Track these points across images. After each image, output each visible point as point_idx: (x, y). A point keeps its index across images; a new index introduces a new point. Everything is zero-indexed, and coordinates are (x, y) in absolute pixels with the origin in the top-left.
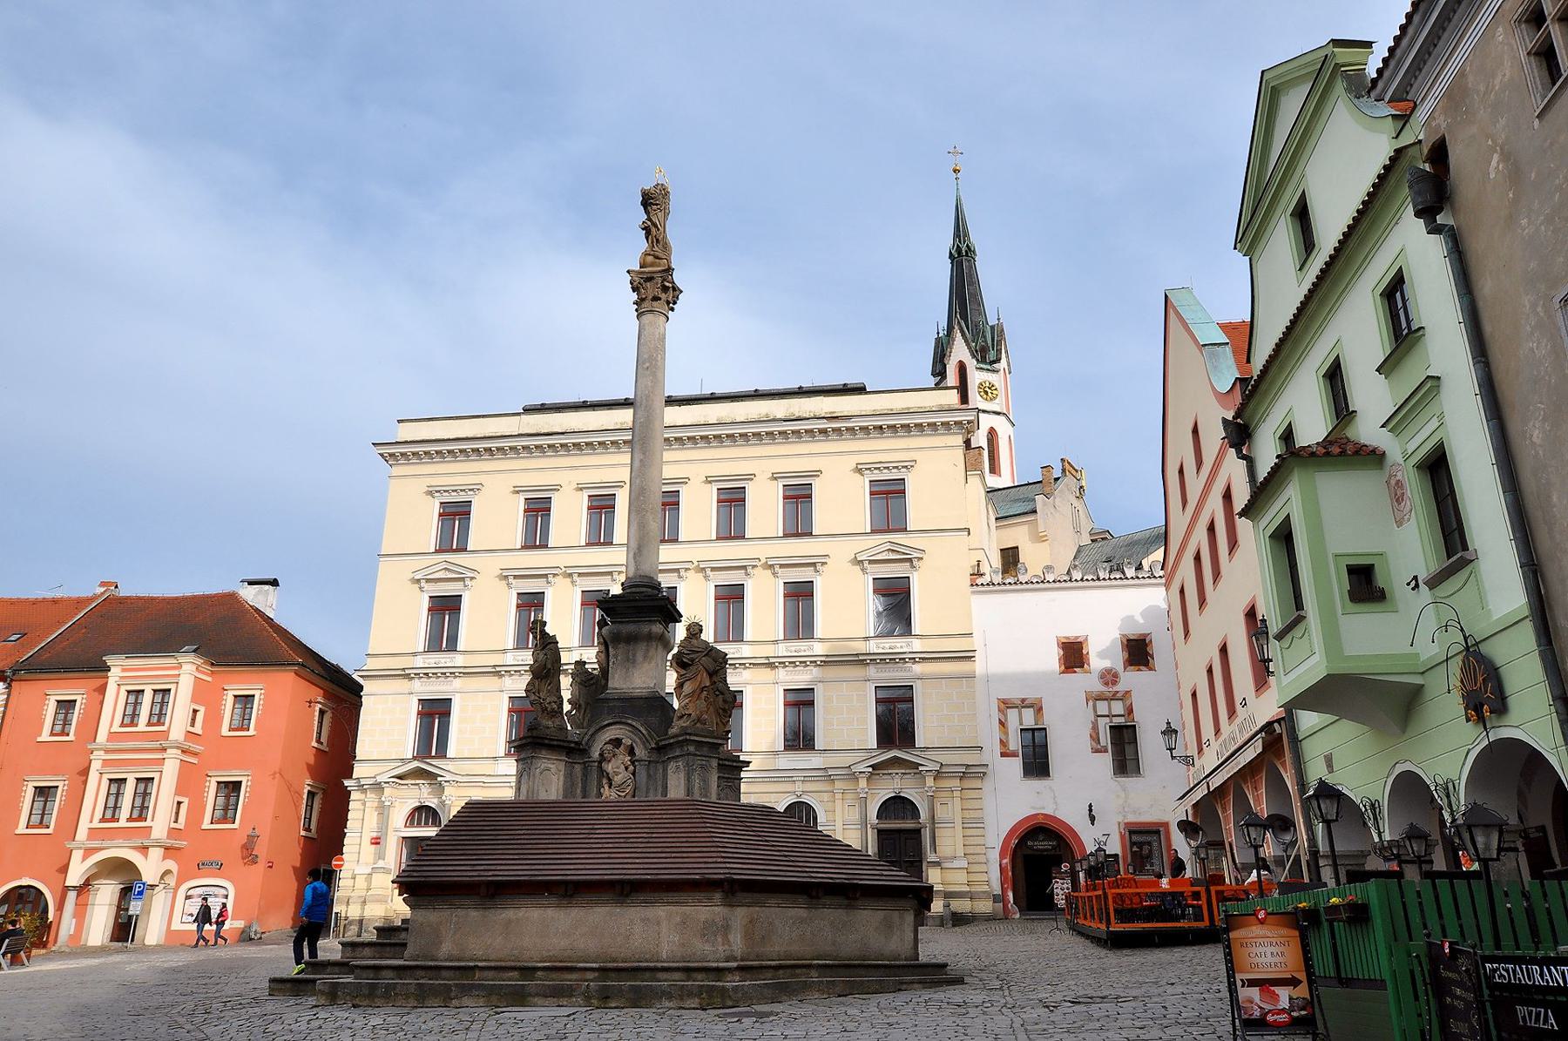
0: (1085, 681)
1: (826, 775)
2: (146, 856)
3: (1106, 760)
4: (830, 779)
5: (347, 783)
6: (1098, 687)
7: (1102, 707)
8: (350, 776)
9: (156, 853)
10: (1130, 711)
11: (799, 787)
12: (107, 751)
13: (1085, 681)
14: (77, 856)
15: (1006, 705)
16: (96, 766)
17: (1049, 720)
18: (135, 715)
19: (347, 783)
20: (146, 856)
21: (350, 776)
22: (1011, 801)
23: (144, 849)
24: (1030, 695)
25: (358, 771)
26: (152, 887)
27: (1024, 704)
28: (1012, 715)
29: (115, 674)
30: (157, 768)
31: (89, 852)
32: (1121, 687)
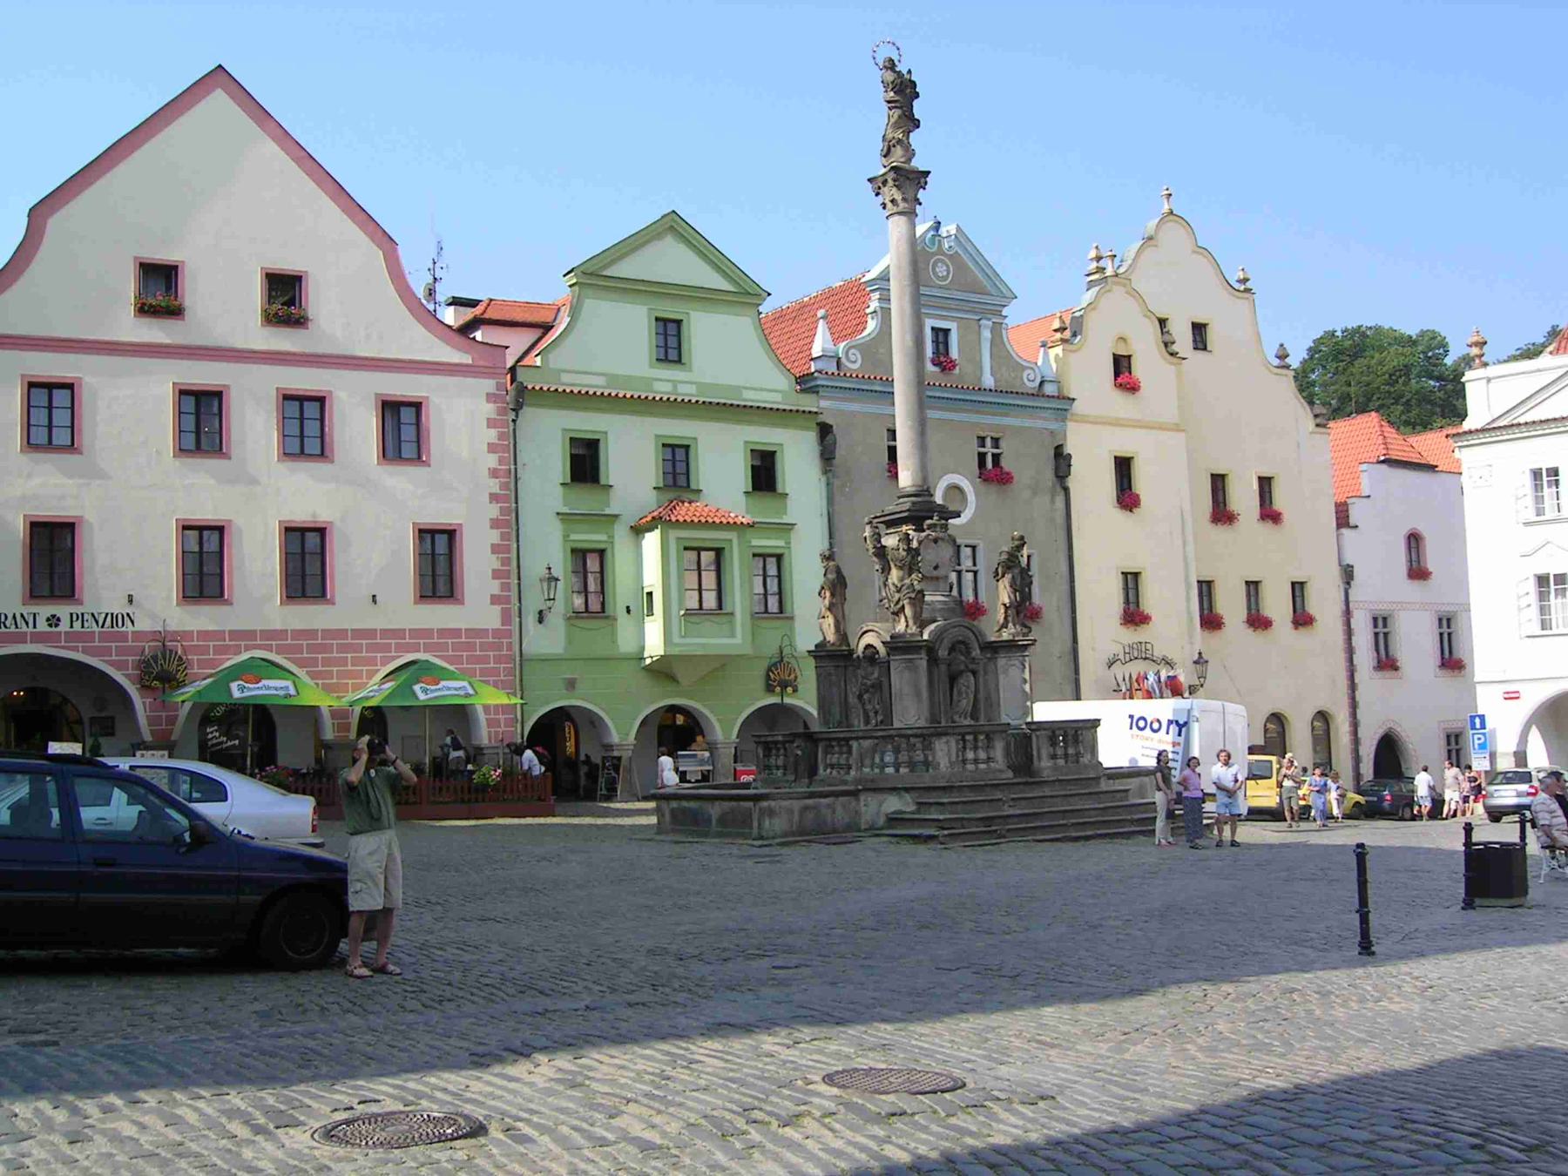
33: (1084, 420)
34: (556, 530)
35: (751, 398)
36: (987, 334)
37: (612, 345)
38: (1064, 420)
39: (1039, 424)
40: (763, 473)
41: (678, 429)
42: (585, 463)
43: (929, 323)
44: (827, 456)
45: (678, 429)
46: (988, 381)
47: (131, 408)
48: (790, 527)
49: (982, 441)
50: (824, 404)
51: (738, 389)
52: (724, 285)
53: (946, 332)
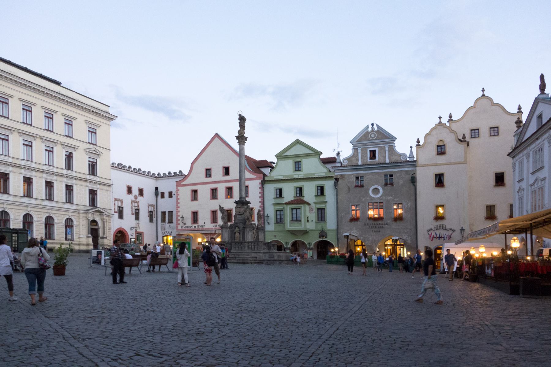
0: (131, 197)
1: (78, 211)
3: (134, 216)
4: (79, 213)
6: (134, 199)
7: (133, 203)
10: (138, 206)
11: (70, 214)
13: (131, 197)
15: (116, 199)
17: (124, 205)
22: (115, 224)
24: (121, 198)
27: (119, 200)
28: (116, 202)
32: (137, 200)
33: (423, 166)
34: (273, 207)
35: (317, 175)
36: (387, 149)
37: (285, 169)
38: (416, 167)
39: (406, 169)
40: (321, 191)
41: (299, 184)
42: (280, 193)
43: (369, 150)
44: (336, 185)
45: (299, 184)
46: (387, 161)
47: (204, 192)
48: (326, 202)
49: (386, 176)
50: (336, 174)
51: (314, 174)
52: (312, 152)
53: (375, 151)
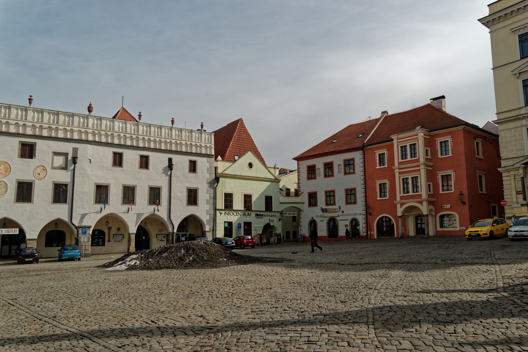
2: (422, 204)
5: (499, 169)
8: (500, 167)
9: (425, 204)
12: (399, 169)
14: (399, 206)
16: (397, 175)
18: (406, 155)
19: (499, 169)
20: (422, 204)
21: (500, 167)
23: (421, 203)
25: (503, 163)
26: (427, 215)
29: (395, 141)
30: (419, 173)
31: (402, 205)
